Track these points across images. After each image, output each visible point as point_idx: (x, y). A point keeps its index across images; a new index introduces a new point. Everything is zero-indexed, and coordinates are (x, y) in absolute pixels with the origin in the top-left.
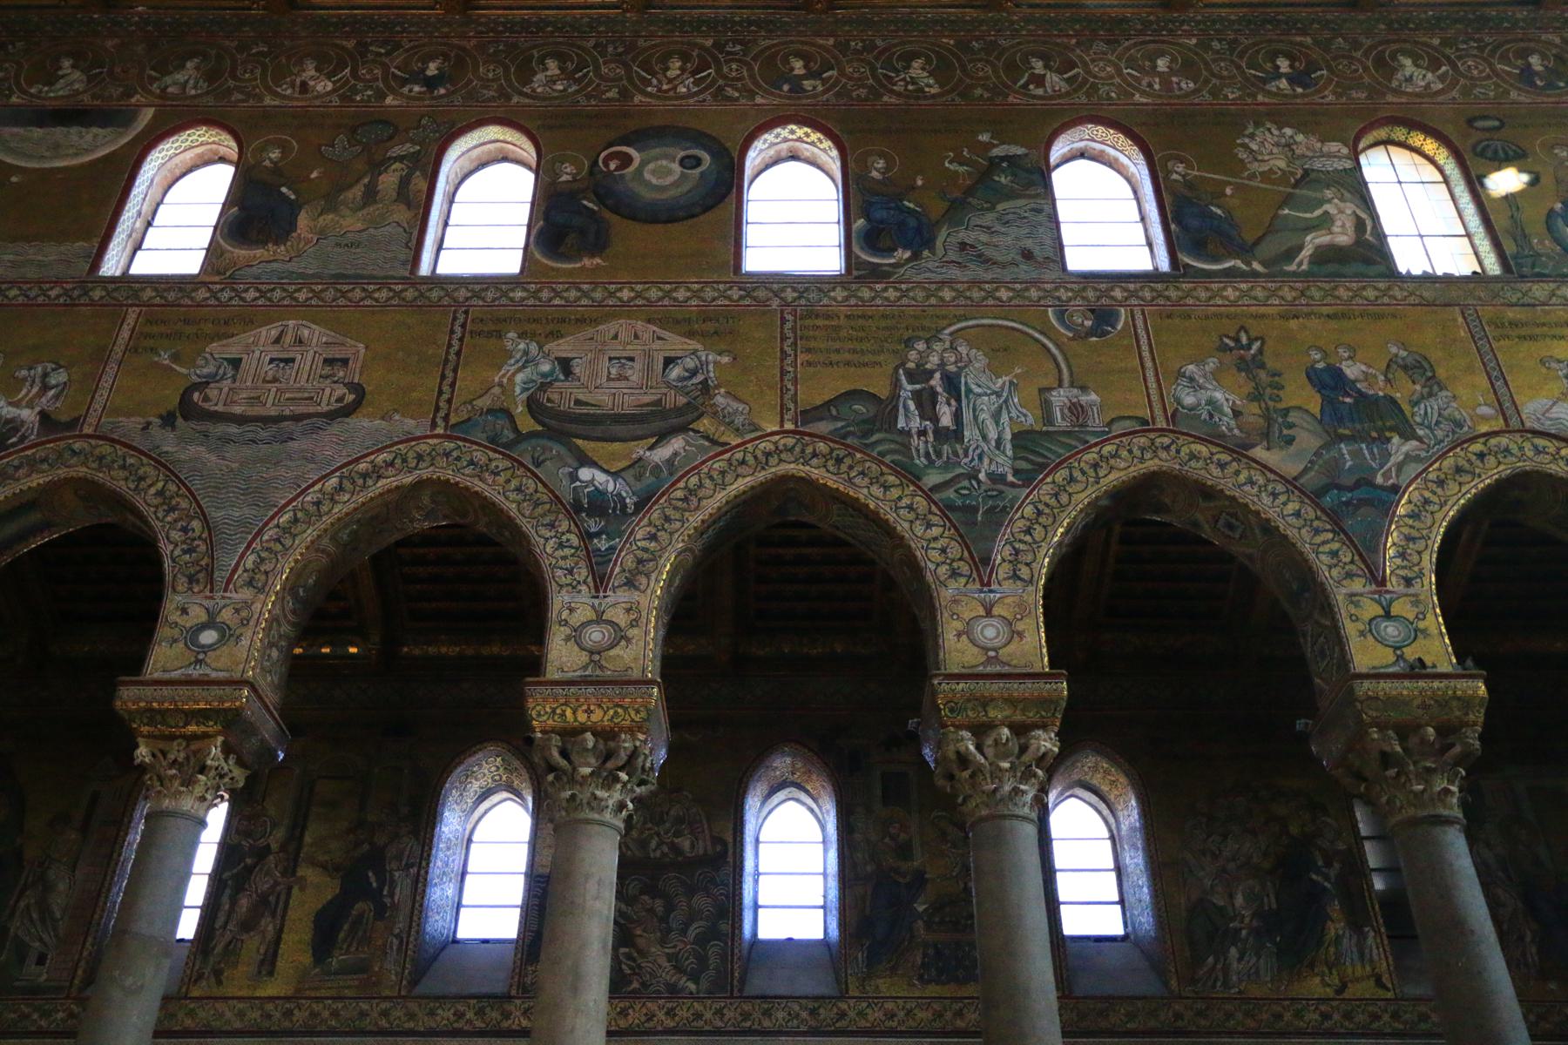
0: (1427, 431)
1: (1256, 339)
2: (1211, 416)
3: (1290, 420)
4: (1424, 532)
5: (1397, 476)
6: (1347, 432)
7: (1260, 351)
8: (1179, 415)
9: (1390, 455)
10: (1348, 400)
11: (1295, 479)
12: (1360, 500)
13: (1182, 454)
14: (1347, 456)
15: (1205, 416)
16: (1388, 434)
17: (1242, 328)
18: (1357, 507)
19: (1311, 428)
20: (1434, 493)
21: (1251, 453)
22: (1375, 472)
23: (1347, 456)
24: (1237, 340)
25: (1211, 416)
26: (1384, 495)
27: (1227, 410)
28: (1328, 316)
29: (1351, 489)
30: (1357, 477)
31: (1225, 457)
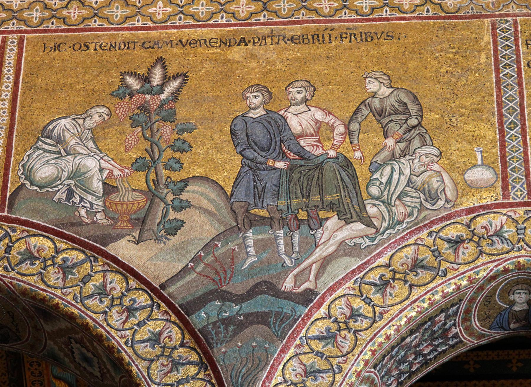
0: (383, 208)
1: (175, 78)
2: (70, 193)
3: (185, 196)
4: (335, 362)
5: (317, 277)
6: (264, 213)
7: (175, 95)
8: (22, 193)
9: (317, 247)
10: (280, 165)
11: (163, 286)
12: (247, 316)
13: (14, 253)
14: (251, 250)
15: (61, 195)
16: (322, 214)
17: (161, 61)
18: (241, 326)
19: (211, 208)
20: (368, 301)
21: (111, 249)
22: (286, 270)
23: (251, 250)
24: (146, 79)
25: (70, 193)
26: (287, 307)
27: (97, 186)
28: (292, 39)
29: (241, 299)
30: (252, 283)
31: (76, 256)
